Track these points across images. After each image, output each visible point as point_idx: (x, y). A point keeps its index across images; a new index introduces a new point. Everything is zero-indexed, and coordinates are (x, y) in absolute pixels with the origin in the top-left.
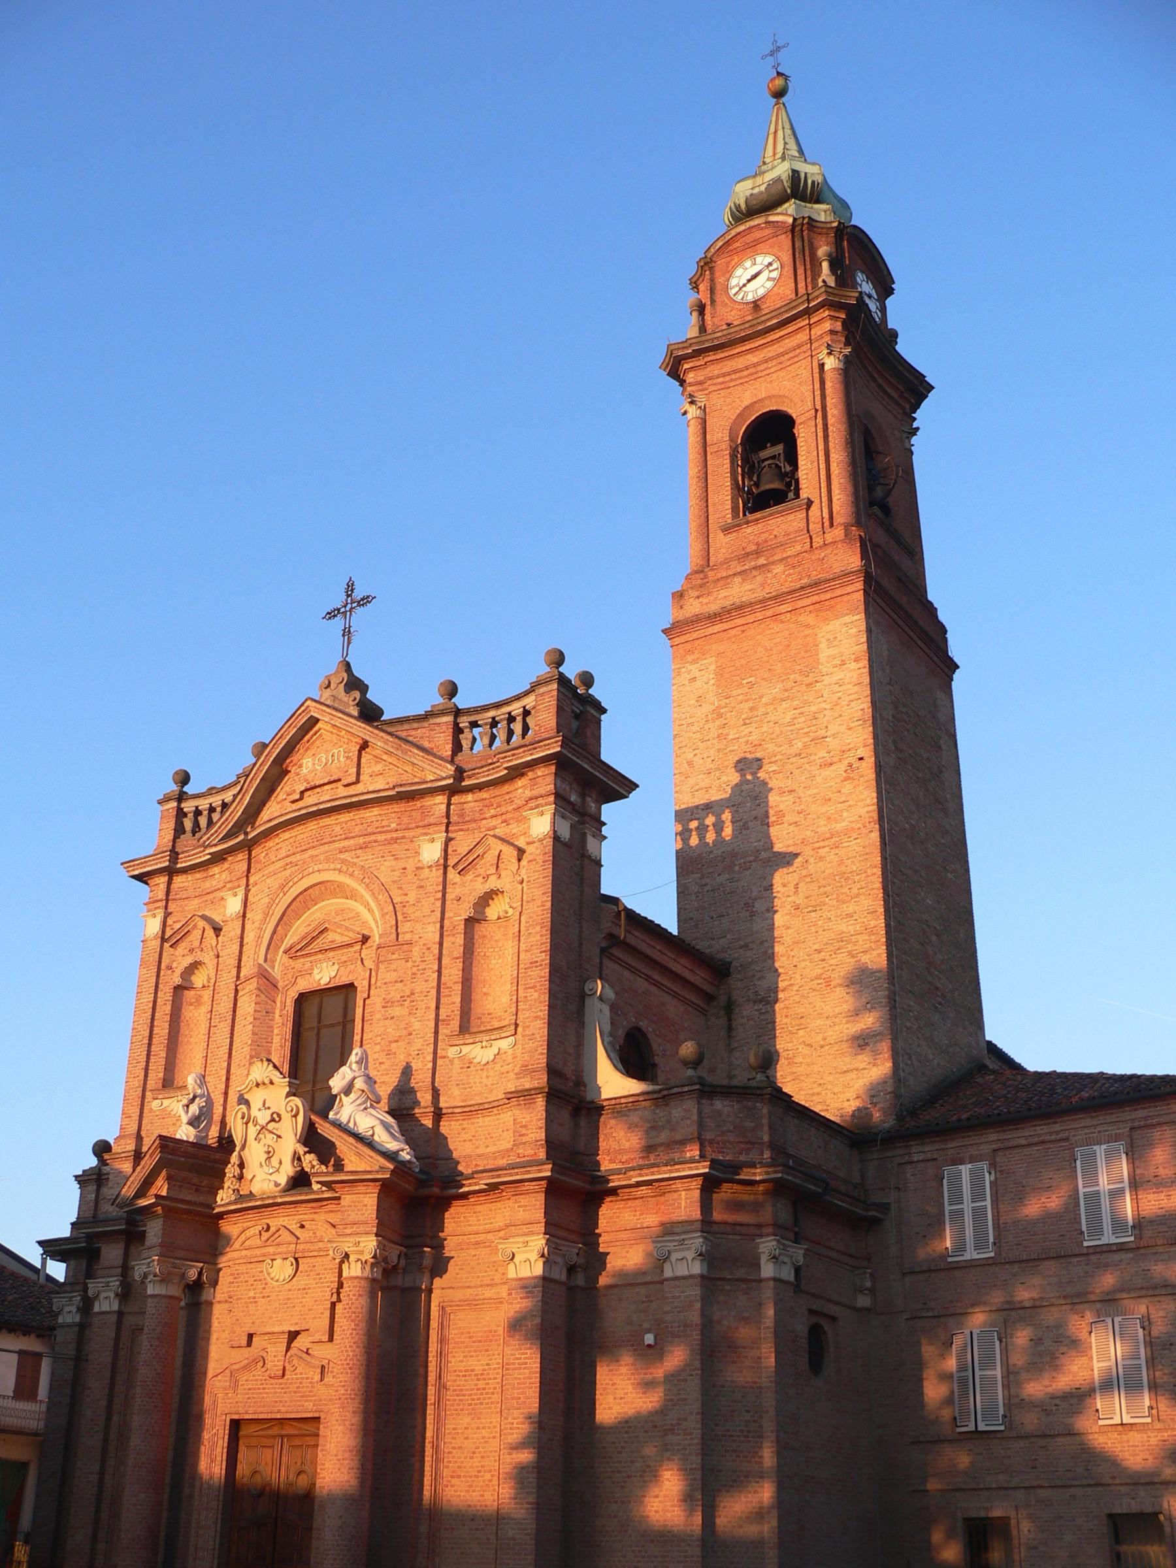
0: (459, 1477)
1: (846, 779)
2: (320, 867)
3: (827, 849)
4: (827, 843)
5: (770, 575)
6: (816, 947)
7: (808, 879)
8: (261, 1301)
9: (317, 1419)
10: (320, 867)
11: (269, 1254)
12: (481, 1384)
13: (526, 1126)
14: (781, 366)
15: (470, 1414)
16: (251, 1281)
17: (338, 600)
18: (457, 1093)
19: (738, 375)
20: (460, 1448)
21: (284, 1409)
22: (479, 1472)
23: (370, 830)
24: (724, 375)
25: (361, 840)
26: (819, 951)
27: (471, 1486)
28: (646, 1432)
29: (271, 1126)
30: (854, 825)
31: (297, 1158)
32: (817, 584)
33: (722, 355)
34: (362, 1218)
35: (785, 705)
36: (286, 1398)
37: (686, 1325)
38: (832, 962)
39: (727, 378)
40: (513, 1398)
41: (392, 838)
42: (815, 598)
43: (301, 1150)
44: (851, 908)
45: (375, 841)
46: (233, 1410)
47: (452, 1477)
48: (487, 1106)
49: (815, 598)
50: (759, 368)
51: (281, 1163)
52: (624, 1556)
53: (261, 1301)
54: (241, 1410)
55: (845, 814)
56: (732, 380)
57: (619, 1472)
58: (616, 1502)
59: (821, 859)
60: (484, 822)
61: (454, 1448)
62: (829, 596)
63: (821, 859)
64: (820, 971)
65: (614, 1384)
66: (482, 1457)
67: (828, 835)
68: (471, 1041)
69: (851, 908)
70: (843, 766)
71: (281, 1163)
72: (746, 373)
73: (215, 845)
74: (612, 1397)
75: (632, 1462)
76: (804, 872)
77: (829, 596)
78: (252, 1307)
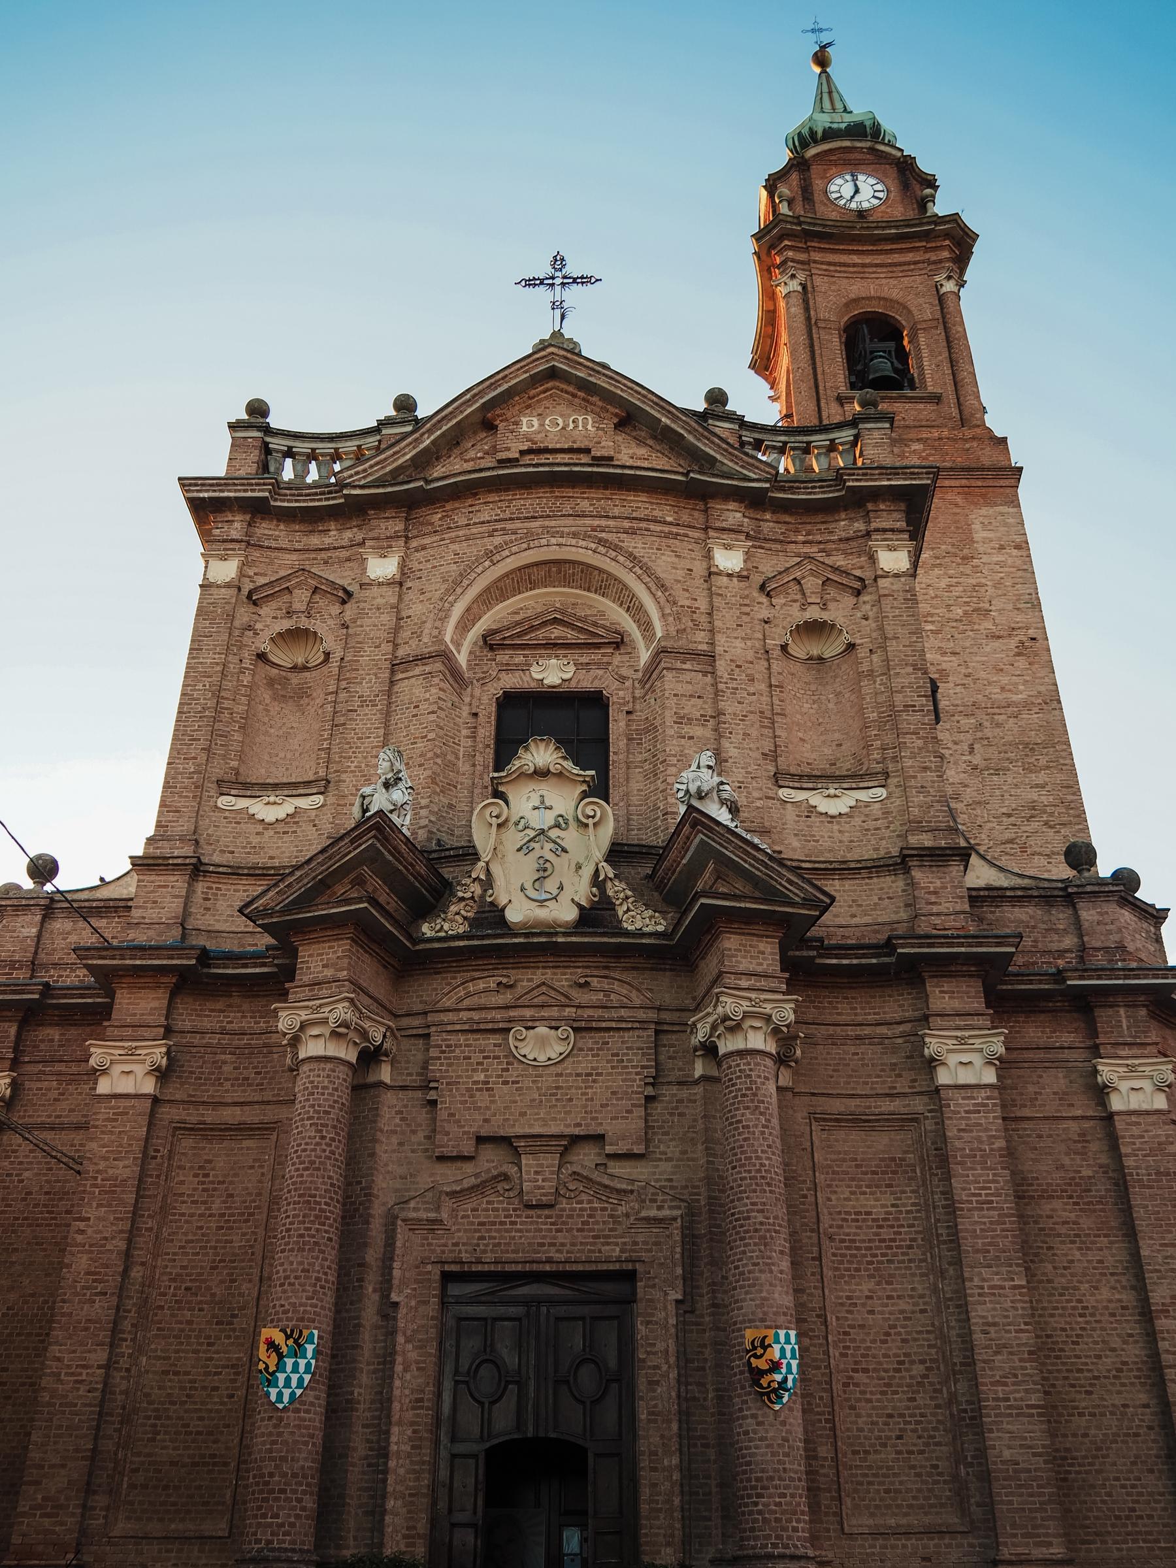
0: (865, 1371)
1: (1019, 654)
2: (561, 540)
3: (1003, 717)
4: (1003, 711)
5: (907, 449)
6: (1004, 810)
7: (986, 742)
8: (501, 1090)
9: (629, 1276)
10: (561, 540)
11: (522, 1020)
12: (886, 1233)
13: (935, 893)
14: (890, 275)
15: (871, 1276)
16: (477, 1057)
17: (543, 269)
18: (796, 844)
19: (843, 269)
20: (862, 1326)
21: (558, 1256)
22: (901, 1363)
23: (634, 515)
24: (829, 264)
25: (626, 524)
26: (1009, 815)
27: (888, 1385)
28: (1113, 1315)
29: (554, 833)
30: (1033, 699)
31: (597, 881)
32: (969, 469)
33: (827, 246)
34: (759, 969)
35: (937, 571)
36: (561, 1238)
37: (1158, 1173)
38: (1024, 828)
39: (832, 268)
40: (977, 1251)
41: (670, 533)
42: (964, 482)
43: (608, 870)
44: (1042, 777)
45: (647, 530)
46: (448, 1256)
47: (855, 1371)
48: (853, 865)
49: (964, 482)
50: (866, 270)
51: (561, 888)
52: (1109, 1495)
53: (501, 1090)
54: (465, 1256)
55: (1021, 687)
56: (836, 271)
57: (1080, 1371)
58: (1081, 1415)
59: (998, 725)
60: (793, 546)
61: (852, 1327)
62: (979, 483)
63: (998, 725)
64: (1014, 835)
65: (1049, 1248)
66: (904, 1341)
67: (1004, 704)
68: (810, 785)
69: (1042, 777)
70: (1013, 643)
71: (561, 888)
72: (851, 269)
73: (362, 487)
74: (1050, 1266)
75: (1099, 1357)
76: (979, 734)
77: (979, 483)
78: (482, 1099)
